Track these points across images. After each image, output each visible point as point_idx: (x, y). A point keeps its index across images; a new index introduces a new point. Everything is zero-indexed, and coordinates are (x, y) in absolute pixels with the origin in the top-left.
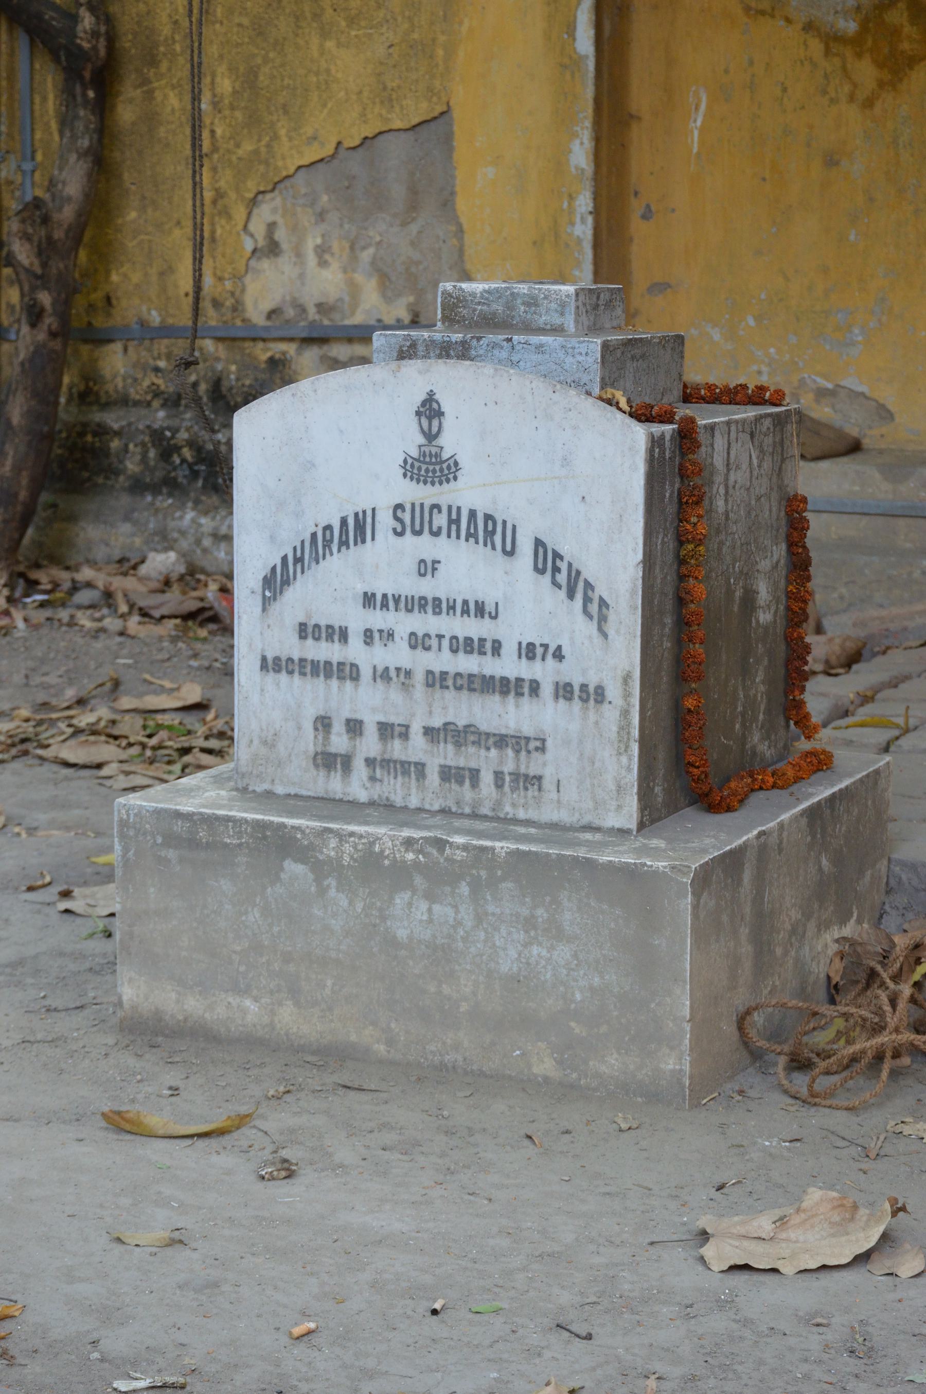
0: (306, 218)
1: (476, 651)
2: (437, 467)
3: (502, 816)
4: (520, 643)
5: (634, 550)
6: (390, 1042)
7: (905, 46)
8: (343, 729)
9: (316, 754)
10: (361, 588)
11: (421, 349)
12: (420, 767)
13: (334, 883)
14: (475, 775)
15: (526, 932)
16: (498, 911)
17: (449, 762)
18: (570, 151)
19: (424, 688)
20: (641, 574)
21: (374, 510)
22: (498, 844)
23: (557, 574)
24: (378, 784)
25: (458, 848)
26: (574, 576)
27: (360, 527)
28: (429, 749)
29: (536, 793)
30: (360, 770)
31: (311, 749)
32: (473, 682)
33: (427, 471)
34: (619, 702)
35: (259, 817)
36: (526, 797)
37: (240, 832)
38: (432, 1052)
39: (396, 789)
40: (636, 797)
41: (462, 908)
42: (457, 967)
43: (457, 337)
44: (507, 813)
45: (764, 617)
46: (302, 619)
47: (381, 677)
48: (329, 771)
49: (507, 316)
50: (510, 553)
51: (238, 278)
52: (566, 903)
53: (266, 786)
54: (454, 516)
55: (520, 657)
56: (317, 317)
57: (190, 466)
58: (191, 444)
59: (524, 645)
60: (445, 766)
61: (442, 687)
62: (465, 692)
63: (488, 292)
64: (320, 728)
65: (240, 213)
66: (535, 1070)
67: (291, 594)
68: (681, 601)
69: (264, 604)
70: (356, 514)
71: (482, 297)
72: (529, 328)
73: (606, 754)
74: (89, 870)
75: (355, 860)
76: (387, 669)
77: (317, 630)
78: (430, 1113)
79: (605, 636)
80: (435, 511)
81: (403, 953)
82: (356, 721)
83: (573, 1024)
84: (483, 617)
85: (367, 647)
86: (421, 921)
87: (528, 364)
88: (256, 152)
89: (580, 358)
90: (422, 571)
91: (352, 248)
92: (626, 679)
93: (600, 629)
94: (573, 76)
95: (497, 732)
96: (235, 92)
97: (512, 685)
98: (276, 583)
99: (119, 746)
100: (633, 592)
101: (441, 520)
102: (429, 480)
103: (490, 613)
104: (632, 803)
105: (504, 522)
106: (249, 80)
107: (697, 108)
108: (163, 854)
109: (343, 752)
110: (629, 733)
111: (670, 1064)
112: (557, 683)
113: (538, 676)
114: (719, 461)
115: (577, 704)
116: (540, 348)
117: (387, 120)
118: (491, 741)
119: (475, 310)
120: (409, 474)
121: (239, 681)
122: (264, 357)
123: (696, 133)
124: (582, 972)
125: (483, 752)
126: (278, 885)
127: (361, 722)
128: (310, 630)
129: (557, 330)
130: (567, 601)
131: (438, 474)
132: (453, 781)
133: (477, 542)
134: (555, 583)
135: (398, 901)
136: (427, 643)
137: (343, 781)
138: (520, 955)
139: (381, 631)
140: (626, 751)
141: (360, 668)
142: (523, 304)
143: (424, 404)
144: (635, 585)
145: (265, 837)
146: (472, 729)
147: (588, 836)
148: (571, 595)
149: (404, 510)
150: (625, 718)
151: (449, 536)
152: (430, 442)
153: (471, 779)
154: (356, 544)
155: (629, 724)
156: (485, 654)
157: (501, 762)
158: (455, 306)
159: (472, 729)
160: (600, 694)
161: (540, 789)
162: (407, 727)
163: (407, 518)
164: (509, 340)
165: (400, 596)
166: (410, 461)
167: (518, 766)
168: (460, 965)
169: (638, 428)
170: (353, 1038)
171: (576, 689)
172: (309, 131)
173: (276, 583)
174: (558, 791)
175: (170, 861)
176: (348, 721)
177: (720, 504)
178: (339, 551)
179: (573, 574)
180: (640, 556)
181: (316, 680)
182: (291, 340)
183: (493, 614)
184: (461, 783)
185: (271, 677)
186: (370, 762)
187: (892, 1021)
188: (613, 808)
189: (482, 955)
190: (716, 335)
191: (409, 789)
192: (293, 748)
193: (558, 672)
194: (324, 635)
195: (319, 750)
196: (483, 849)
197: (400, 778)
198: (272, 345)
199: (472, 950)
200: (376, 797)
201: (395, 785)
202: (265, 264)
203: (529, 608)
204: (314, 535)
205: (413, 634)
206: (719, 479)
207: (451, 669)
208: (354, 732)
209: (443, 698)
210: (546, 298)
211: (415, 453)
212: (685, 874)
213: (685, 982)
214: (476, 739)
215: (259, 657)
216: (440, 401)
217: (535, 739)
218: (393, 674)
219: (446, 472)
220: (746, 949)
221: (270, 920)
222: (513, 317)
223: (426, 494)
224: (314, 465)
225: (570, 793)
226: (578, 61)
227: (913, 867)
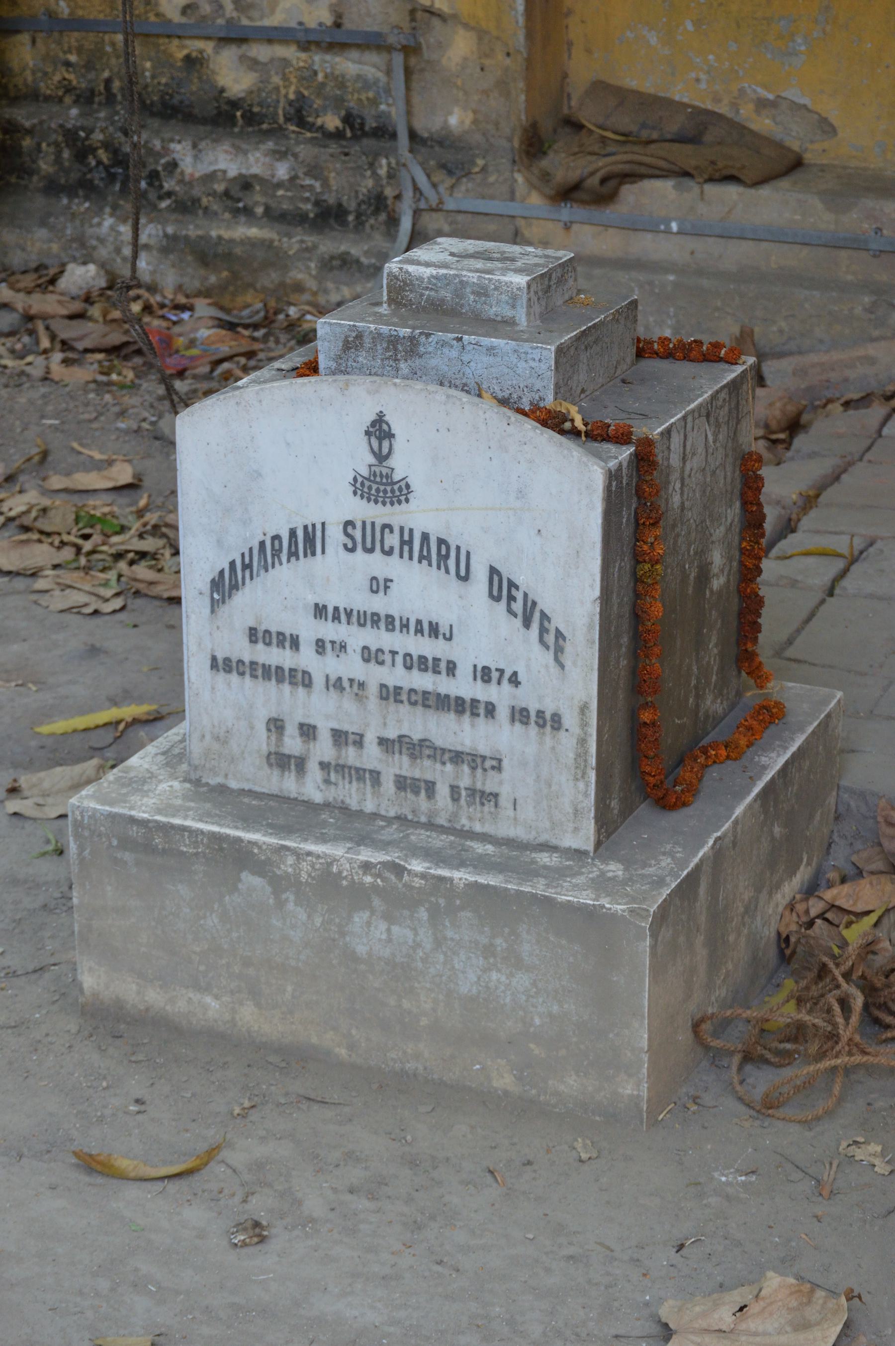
1: (430, 669)
3: (458, 827)
4: (475, 666)
5: (592, 586)
6: (352, 1047)
8: (296, 732)
9: (270, 754)
10: (312, 599)
12: (376, 777)
13: (292, 897)
14: (430, 788)
15: (485, 958)
16: (457, 937)
17: (404, 773)
19: (378, 701)
20: (598, 610)
21: (323, 524)
22: (457, 875)
24: (333, 787)
25: (416, 875)
27: (310, 540)
29: (493, 809)
30: (314, 773)
31: (265, 749)
33: (378, 490)
34: (576, 730)
35: (215, 829)
36: (482, 812)
37: (197, 842)
38: (392, 1059)
39: (351, 794)
40: (593, 821)
41: (421, 931)
42: (416, 985)
44: (463, 826)
45: (717, 584)
46: (252, 624)
47: (334, 686)
48: (283, 771)
49: (457, 304)
50: (465, 578)
52: (524, 935)
53: (219, 780)
54: (406, 537)
55: (475, 679)
56: (235, 14)
57: (107, 168)
58: (107, 145)
59: (479, 668)
60: (400, 776)
61: (396, 701)
63: (436, 277)
64: (273, 730)
66: (495, 1084)
67: (240, 599)
68: (637, 616)
69: (212, 606)
70: (306, 527)
71: (429, 282)
74: (33, 743)
75: (313, 878)
76: (340, 679)
77: (267, 635)
78: (393, 1136)
79: (562, 666)
80: (387, 530)
81: (363, 967)
82: (309, 725)
83: (532, 1046)
84: (437, 637)
85: (319, 657)
86: (380, 940)
87: (479, 365)
89: (533, 364)
90: (375, 588)
92: (583, 709)
93: (556, 659)
97: (467, 705)
98: (224, 586)
99: (51, 544)
100: (590, 627)
101: (393, 540)
102: (380, 499)
103: (444, 635)
104: (589, 827)
105: (458, 548)
108: (119, 855)
109: (297, 754)
110: (586, 761)
111: (628, 1090)
113: (494, 699)
114: (675, 460)
115: (533, 730)
116: (491, 350)
118: (447, 756)
120: (359, 492)
122: (180, 55)
124: (541, 1000)
125: (438, 766)
126: (236, 894)
127: (314, 727)
128: (260, 635)
130: (523, 630)
131: (389, 494)
133: (430, 565)
134: (510, 611)
135: (356, 919)
136: (380, 659)
137: (297, 781)
138: (479, 979)
139: (333, 643)
140: (583, 777)
141: (313, 676)
142: (473, 293)
143: (373, 424)
144: (592, 620)
145: (221, 849)
146: (427, 743)
147: (544, 858)
148: (527, 623)
149: (354, 527)
150: (582, 745)
151: (401, 556)
152: (381, 462)
153: (426, 790)
154: (305, 556)
155: (586, 753)
156: (439, 673)
157: (457, 777)
158: (401, 289)
159: (427, 743)
160: (557, 722)
161: (496, 805)
162: (362, 736)
164: (460, 339)
166: (360, 479)
168: (419, 982)
169: (595, 467)
170: (314, 1040)
171: (533, 714)
173: (224, 586)
175: (126, 863)
176: (301, 726)
177: (676, 499)
178: (289, 561)
179: (529, 604)
180: (597, 593)
181: (267, 683)
182: (208, 38)
183: (448, 636)
184: (417, 793)
185: (221, 676)
186: (324, 766)
187: (845, 1033)
188: (570, 830)
189: (441, 976)
190: (653, 39)
191: (364, 794)
193: (514, 697)
194: (274, 641)
195: (273, 750)
196: (441, 879)
197: (354, 783)
198: (188, 42)
199: (432, 970)
200: (331, 799)
203: (483, 633)
204: (262, 544)
205: (365, 648)
206: (675, 476)
208: (308, 736)
209: (398, 712)
210: (496, 289)
211: (365, 472)
212: (644, 918)
213: (643, 1017)
215: (209, 657)
216: (390, 423)
218: (346, 684)
220: (702, 953)
221: (228, 926)
222: (462, 306)
223: (377, 513)
224: (260, 475)
225: (527, 812)
227: (862, 795)
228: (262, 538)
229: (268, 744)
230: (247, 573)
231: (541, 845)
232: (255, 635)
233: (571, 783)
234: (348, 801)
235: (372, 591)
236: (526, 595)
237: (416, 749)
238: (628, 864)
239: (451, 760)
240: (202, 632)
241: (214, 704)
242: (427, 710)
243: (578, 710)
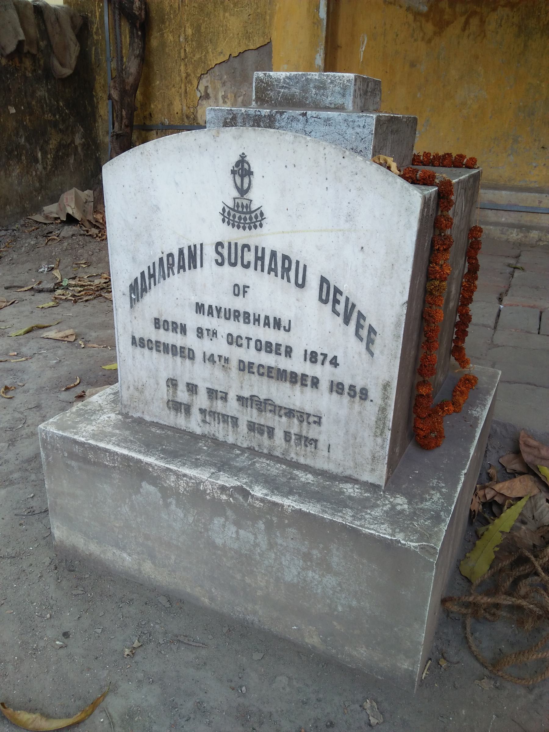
0: (219, 84)
2: (248, 216)
3: (289, 459)
4: (306, 351)
5: (402, 293)
6: (212, 599)
7: (446, 17)
8: (185, 389)
9: (169, 401)
10: (194, 299)
11: (239, 120)
12: (235, 421)
13: (174, 502)
14: (271, 431)
15: (304, 561)
16: (285, 544)
17: (254, 420)
18: (316, 59)
19: (237, 371)
20: (405, 311)
21: (202, 245)
23: (337, 305)
25: (257, 499)
26: (350, 308)
28: (241, 409)
29: (313, 450)
30: (196, 416)
31: (166, 398)
32: (271, 372)
33: (240, 218)
34: (379, 402)
35: (125, 452)
36: (305, 451)
37: (114, 460)
38: (238, 611)
39: (220, 431)
40: (386, 466)
41: (260, 537)
42: (255, 569)
43: (265, 112)
44: (292, 458)
47: (208, 360)
48: (177, 413)
49: (303, 97)
50: (301, 286)
51: (195, 107)
52: (334, 551)
54: (260, 254)
55: (305, 360)
59: (309, 353)
61: (249, 372)
62: (265, 378)
63: (289, 78)
64: (171, 386)
65: (195, 82)
66: (307, 640)
67: (148, 298)
69: (131, 303)
70: (190, 247)
71: (285, 82)
72: (317, 107)
73: (366, 434)
74: (100, 373)
75: (188, 492)
77: (166, 324)
78: (233, 685)
79: (372, 354)
80: (246, 249)
81: (219, 552)
83: (335, 623)
84: (279, 329)
85: (199, 339)
86: (231, 537)
87: (318, 134)
88: (201, 58)
89: (358, 130)
90: (236, 292)
91: (235, 96)
92: (386, 386)
93: (368, 348)
94: (318, 28)
95: (287, 407)
96: (193, 34)
97: (299, 378)
98: (138, 289)
100: (398, 325)
101: (250, 257)
102: (242, 225)
103: (285, 327)
105: (298, 262)
106: (198, 29)
107: (363, 43)
108: (69, 462)
110: (384, 424)
111: (406, 665)
112: (332, 381)
113: (318, 375)
115: (346, 398)
116: (327, 122)
117: (248, 45)
118: (283, 412)
119: (279, 92)
120: (227, 220)
121: (119, 350)
123: (362, 53)
124: (344, 596)
125: (277, 418)
126: (139, 495)
127: (196, 386)
129: (340, 108)
130: (343, 325)
131: (248, 221)
132: (256, 432)
133: (276, 275)
134: (334, 311)
135: (216, 522)
136: (240, 342)
137: (186, 419)
138: (299, 573)
139: (208, 330)
140: (381, 435)
142: (315, 87)
143: (237, 164)
144: (399, 320)
145: (129, 466)
146: (270, 402)
147: (350, 489)
148: (347, 321)
149: (223, 247)
150: (383, 413)
151: (256, 269)
152: (242, 196)
153: (268, 433)
154: (190, 268)
156: (280, 354)
158: (266, 89)
159: (270, 402)
160: (364, 394)
161: (316, 448)
162: (226, 394)
163: (225, 252)
164: (304, 115)
165: (221, 308)
166: (227, 210)
167: (301, 431)
168: (257, 569)
169: (415, 192)
170: (188, 590)
172: (219, 50)
173: (138, 289)
174: (329, 452)
175: (73, 467)
176: (188, 384)
178: (179, 272)
180: (406, 298)
181: (166, 355)
184: (262, 434)
186: (202, 411)
188: (368, 469)
189: (273, 567)
191: (227, 431)
192: (154, 395)
194: (170, 328)
196: (275, 504)
197: (221, 424)
199: (266, 562)
200: (206, 433)
201: (218, 428)
202: (204, 102)
203: (313, 326)
204: (161, 260)
205: (229, 335)
207: (257, 362)
208: (192, 391)
209: (250, 379)
211: (231, 204)
212: (433, 555)
213: (423, 622)
214: (273, 409)
215: (131, 337)
216: (250, 162)
217: (313, 415)
218: (216, 359)
219: (254, 220)
221: (135, 514)
222: (307, 98)
223: (239, 236)
224: (158, 208)
225: (337, 454)
226: (320, 21)
228: (160, 255)
229: (168, 395)
230: (152, 280)
231: (346, 477)
232: (158, 323)
233: (372, 438)
234: (217, 435)
235: (235, 295)
236: (347, 299)
237: (262, 405)
238: (410, 498)
239: (286, 414)
240: (128, 320)
241: (136, 367)
242: (270, 379)
243: (381, 387)
